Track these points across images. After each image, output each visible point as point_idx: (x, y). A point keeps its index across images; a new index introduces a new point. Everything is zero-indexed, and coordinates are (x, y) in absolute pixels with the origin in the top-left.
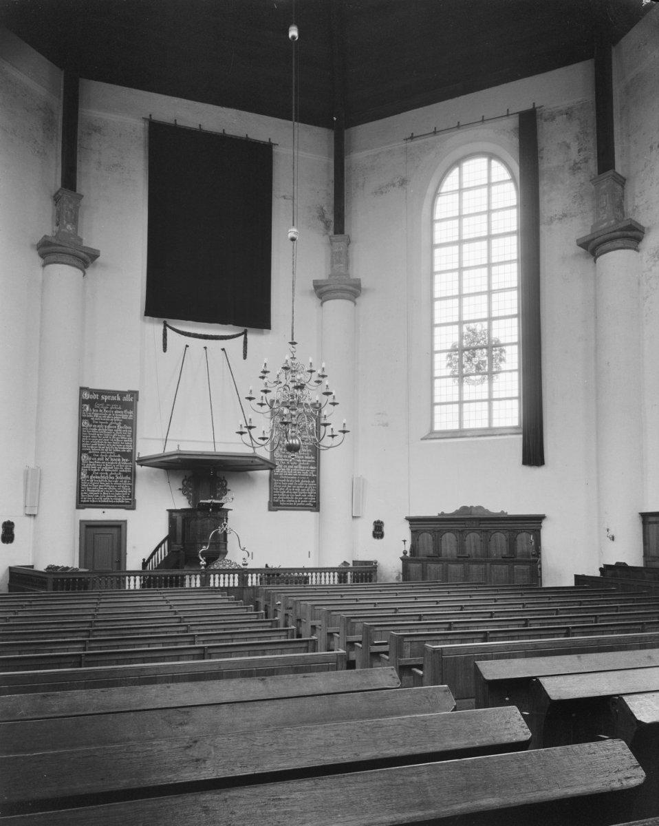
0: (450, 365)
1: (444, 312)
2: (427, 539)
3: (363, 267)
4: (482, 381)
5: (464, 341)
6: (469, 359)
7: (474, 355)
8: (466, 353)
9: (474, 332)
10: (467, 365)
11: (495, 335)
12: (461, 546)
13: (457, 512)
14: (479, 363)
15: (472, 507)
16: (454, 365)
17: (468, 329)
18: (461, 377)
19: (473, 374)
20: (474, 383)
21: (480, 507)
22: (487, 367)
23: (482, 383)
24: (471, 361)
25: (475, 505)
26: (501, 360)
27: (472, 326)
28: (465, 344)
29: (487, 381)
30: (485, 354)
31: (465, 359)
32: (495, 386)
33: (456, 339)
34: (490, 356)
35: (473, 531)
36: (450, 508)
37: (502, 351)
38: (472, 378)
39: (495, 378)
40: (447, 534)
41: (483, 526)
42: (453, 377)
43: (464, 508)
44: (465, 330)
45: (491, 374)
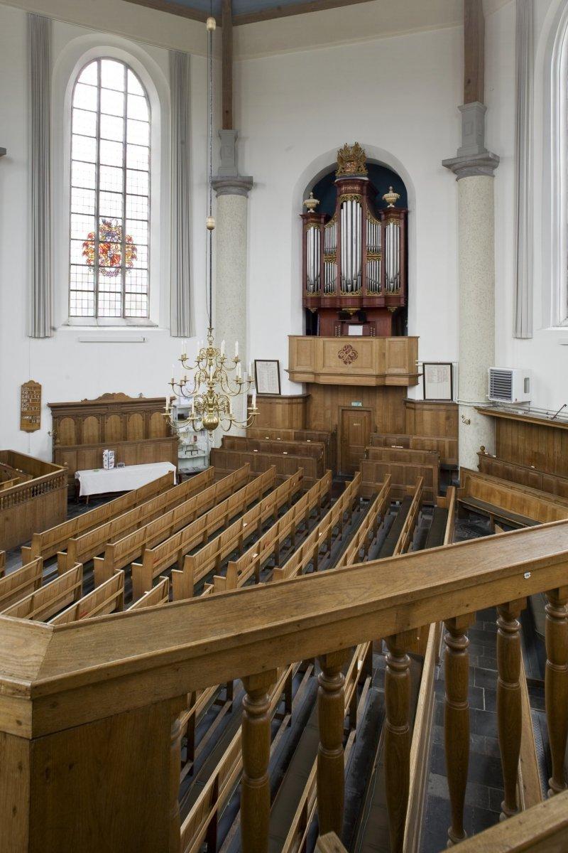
0: (85, 253)
1: (81, 201)
2: (68, 424)
3: (501, 139)
4: (116, 274)
5: (100, 233)
6: (105, 252)
7: (109, 247)
8: (102, 245)
9: (109, 225)
10: (103, 257)
11: (128, 232)
12: (102, 429)
13: (100, 398)
14: (113, 257)
15: (114, 394)
16: (90, 254)
17: (104, 222)
18: (97, 268)
19: (108, 267)
20: (109, 274)
21: (122, 394)
22: (120, 262)
23: (116, 275)
24: (106, 253)
25: (117, 392)
26: (133, 257)
27: (108, 220)
28: (100, 236)
29: (120, 275)
30: (119, 249)
31: (100, 251)
32: (128, 280)
33: (93, 229)
34: (123, 250)
35: (114, 413)
36: (93, 395)
37: (134, 249)
38: (107, 269)
39: (127, 272)
40: (90, 418)
41: (124, 408)
42: (89, 266)
43: (107, 396)
44: (101, 222)
45: (123, 270)
